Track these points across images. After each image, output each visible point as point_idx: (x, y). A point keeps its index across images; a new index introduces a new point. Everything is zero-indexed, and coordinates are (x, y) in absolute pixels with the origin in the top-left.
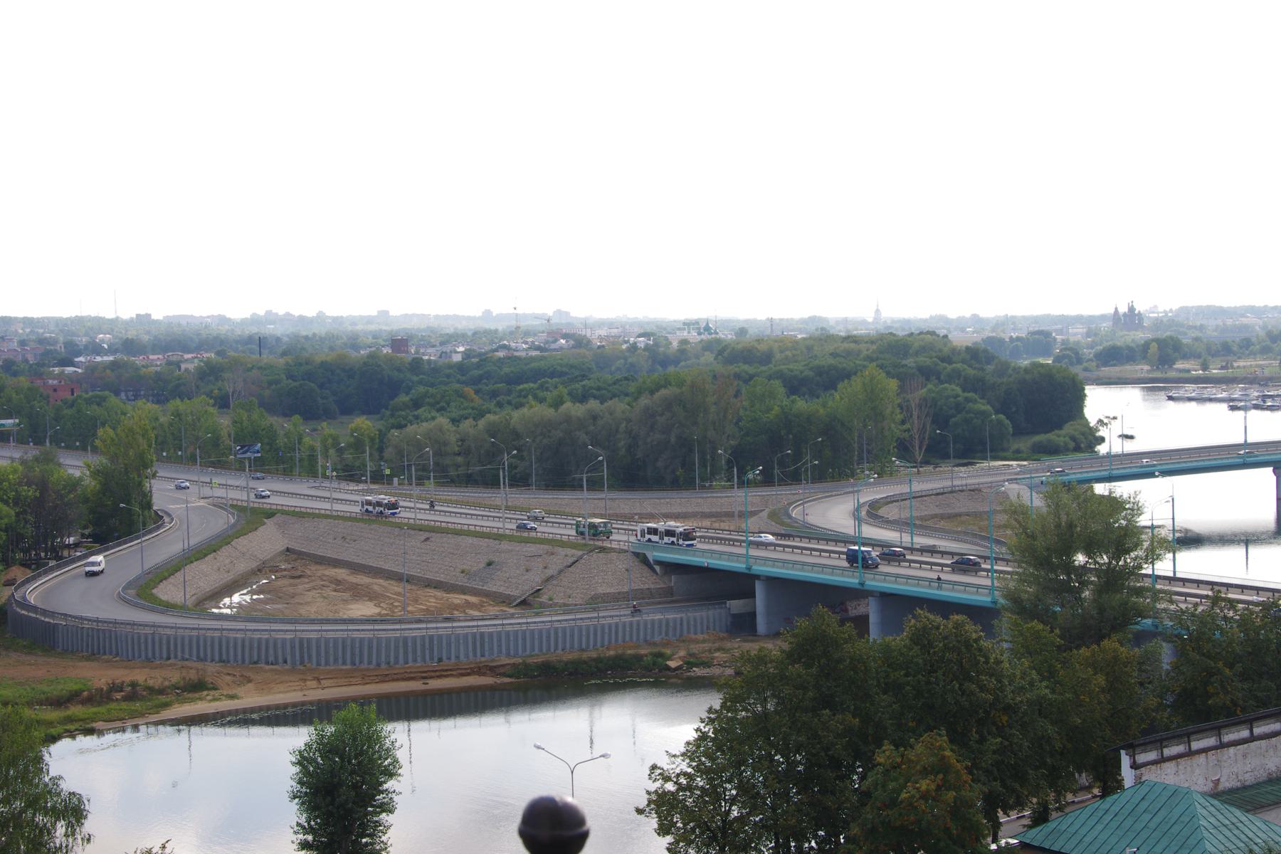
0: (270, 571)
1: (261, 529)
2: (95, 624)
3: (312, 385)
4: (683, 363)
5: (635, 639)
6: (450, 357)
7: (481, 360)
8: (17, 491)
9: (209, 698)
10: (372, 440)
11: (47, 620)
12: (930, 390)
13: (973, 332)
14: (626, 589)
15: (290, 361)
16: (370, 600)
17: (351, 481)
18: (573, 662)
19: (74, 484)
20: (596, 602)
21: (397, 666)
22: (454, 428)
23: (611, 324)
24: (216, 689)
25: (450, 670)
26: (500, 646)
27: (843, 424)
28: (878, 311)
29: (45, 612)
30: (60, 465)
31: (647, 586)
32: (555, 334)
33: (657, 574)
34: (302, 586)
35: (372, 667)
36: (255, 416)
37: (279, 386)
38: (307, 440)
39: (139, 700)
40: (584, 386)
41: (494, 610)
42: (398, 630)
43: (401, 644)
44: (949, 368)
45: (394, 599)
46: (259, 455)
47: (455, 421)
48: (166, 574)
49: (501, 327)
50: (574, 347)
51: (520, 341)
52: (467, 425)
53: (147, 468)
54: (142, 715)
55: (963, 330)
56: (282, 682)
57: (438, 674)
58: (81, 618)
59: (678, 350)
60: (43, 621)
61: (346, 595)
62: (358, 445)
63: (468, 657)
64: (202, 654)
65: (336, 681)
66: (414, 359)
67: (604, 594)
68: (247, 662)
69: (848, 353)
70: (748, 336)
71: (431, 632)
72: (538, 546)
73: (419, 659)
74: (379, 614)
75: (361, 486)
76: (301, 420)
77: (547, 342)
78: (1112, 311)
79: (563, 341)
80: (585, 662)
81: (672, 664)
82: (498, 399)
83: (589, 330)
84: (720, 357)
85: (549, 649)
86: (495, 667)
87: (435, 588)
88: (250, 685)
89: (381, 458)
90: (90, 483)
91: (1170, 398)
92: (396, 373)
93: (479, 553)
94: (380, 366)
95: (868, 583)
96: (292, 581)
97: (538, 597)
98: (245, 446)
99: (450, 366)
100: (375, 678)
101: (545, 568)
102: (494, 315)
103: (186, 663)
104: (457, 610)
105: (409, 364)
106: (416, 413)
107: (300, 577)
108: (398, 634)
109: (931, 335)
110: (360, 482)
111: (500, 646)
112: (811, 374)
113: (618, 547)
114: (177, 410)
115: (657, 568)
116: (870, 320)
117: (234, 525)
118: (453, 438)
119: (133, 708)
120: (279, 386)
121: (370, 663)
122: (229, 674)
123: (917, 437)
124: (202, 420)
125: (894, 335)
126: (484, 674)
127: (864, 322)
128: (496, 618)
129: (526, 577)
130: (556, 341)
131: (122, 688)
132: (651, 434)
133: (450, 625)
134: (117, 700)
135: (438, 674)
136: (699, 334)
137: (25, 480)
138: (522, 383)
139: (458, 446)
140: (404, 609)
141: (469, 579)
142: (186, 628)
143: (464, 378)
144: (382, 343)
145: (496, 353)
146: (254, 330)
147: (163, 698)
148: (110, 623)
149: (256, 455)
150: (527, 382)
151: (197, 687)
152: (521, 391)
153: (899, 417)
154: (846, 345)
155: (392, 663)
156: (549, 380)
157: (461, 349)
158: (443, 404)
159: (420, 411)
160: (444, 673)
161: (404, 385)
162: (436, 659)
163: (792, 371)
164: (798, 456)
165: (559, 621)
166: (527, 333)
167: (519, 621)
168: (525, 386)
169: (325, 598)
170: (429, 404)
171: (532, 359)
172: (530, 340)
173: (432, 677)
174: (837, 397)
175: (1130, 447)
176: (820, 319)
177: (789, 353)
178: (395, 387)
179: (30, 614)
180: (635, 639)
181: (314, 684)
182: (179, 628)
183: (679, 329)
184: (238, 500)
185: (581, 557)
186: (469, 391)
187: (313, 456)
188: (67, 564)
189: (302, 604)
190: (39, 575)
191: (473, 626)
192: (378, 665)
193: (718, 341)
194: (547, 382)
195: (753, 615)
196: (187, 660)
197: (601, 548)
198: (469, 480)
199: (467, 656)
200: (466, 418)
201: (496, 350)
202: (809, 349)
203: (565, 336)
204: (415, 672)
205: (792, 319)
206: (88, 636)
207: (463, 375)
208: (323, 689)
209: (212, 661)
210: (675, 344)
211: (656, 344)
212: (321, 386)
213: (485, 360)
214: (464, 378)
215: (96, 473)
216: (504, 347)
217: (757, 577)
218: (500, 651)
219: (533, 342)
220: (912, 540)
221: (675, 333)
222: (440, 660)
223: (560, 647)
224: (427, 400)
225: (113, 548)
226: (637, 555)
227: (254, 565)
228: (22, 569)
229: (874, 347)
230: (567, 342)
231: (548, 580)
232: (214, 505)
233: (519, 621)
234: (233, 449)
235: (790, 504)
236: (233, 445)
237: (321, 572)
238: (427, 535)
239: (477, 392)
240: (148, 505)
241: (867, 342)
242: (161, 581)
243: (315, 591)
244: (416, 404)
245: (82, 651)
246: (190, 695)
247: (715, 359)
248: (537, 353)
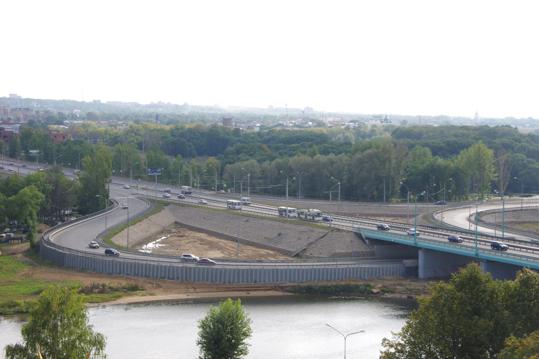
0: (167, 233)
1: (163, 211)
2: (84, 254)
3: (185, 140)
4: (373, 137)
5: (355, 277)
6: (253, 128)
7: (270, 131)
8: (44, 186)
9: (140, 294)
10: (217, 169)
11: (60, 251)
12: (508, 156)
13: (529, 127)
14: (350, 251)
15: (173, 128)
16: (219, 250)
17: (206, 189)
18: (323, 287)
19: (70, 184)
20: (335, 256)
21: (234, 283)
22: (259, 165)
23: (335, 115)
24: (144, 290)
25: (261, 287)
26: (286, 276)
27: (463, 172)
28: (477, 114)
29: (59, 247)
30: (63, 174)
31: (361, 250)
32: (307, 119)
33: (367, 244)
34: (184, 241)
35: (221, 283)
36: (158, 154)
37: (167, 140)
38: (184, 167)
39: (106, 293)
41: (282, 258)
42: (235, 265)
43: (236, 273)
44: (519, 145)
45: (230, 250)
46: (160, 174)
48: (117, 231)
49: (278, 114)
50: (316, 126)
51: (288, 122)
53: (107, 178)
54: (108, 301)
55: (524, 125)
56: (176, 289)
57: (254, 289)
58: (77, 251)
59: (371, 130)
60: (59, 252)
61: (207, 247)
62: (210, 172)
63: (270, 281)
64: (136, 273)
65: (203, 289)
66: (235, 129)
67: (339, 253)
68: (159, 277)
69: (463, 135)
70: (407, 124)
71: (252, 267)
72: (305, 226)
73: (245, 281)
74: (224, 257)
75: (212, 192)
76: (182, 157)
77: (302, 123)
79: (311, 123)
80: (329, 287)
82: (280, 151)
83: (324, 118)
84: (394, 134)
85: (311, 280)
86: (283, 287)
87: (251, 245)
88: (161, 289)
89: (222, 179)
90: (78, 183)
92: (226, 136)
93: (274, 229)
94: (218, 132)
95: (480, 254)
96: (179, 238)
97: (304, 253)
98: (153, 169)
99: (254, 134)
100: (223, 289)
101: (309, 238)
102: (274, 108)
103: (128, 276)
104: (263, 257)
105: (233, 131)
106: (238, 156)
107: (182, 236)
108: (235, 267)
109: (508, 127)
110: (211, 190)
111: (286, 276)
112: (444, 145)
113: (346, 229)
114: (119, 149)
115: (367, 241)
116: (473, 118)
117: (149, 209)
118: (258, 170)
119: (103, 297)
120: (167, 140)
121: (220, 281)
122: (150, 283)
123: (502, 180)
124: (132, 155)
125: (488, 127)
126: (278, 290)
127: (469, 119)
128: (283, 262)
129: (299, 242)
130: (307, 123)
131: (98, 287)
132: (361, 172)
133: (261, 264)
134: (95, 292)
135: (254, 289)
136: (382, 122)
137: (48, 181)
138: (292, 144)
139: (261, 174)
140: (237, 255)
141: (269, 242)
142: (129, 259)
143: (261, 140)
144: (218, 120)
145: (276, 128)
148: (92, 254)
149: (158, 174)
150: (294, 143)
151: (134, 289)
152: (291, 147)
153: (493, 170)
154: (462, 131)
155: (231, 282)
156: (306, 142)
157: (258, 125)
158: (252, 152)
159: (240, 156)
160: (257, 289)
161: (230, 142)
162: (253, 281)
163: (433, 143)
164: (437, 188)
165: (316, 265)
166: (291, 118)
167: (295, 265)
168: (294, 145)
169: (196, 247)
170: (244, 152)
172: (293, 122)
173: (251, 290)
174: (460, 157)
176: (446, 117)
177: (431, 134)
178: (225, 143)
179: (52, 248)
180: (355, 277)
181: (192, 290)
182: (126, 258)
183: (371, 119)
184: (150, 196)
185: (327, 234)
186: (265, 146)
187: (187, 175)
188: (68, 224)
189: (184, 250)
190: (55, 229)
191: (273, 266)
192: (225, 282)
193: (393, 126)
194: (305, 144)
196: (129, 275)
197: (337, 229)
198: (266, 192)
199: (269, 281)
200: (264, 160)
201: (276, 126)
202: (442, 132)
203: (312, 121)
204: (243, 287)
205: (430, 116)
206: (80, 260)
207: (260, 138)
208: (197, 293)
209: (142, 276)
210: (369, 127)
211: (359, 127)
212: (188, 141)
213: (272, 131)
214: (261, 140)
215: (81, 180)
216: (280, 125)
217: (420, 248)
218: (286, 279)
219: (295, 123)
220: (503, 234)
221: (369, 121)
222: (256, 282)
223: (317, 279)
224: (244, 150)
225: (90, 217)
226: (356, 234)
227: (159, 229)
228: (45, 225)
229: (477, 132)
230: (312, 123)
231: (310, 244)
232: (139, 198)
233: (295, 265)
234: (147, 171)
235: (434, 212)
236: (147, 168)
237: (193, 234)
238: (247, 218)
239: (269, 147)
240: (107, 197)
241: (473, 130)
242: (115, 235)
243: (190, 244)
244: (238, 152)
245: (77, 268)
246: (131, 292)
247: (391, 136)
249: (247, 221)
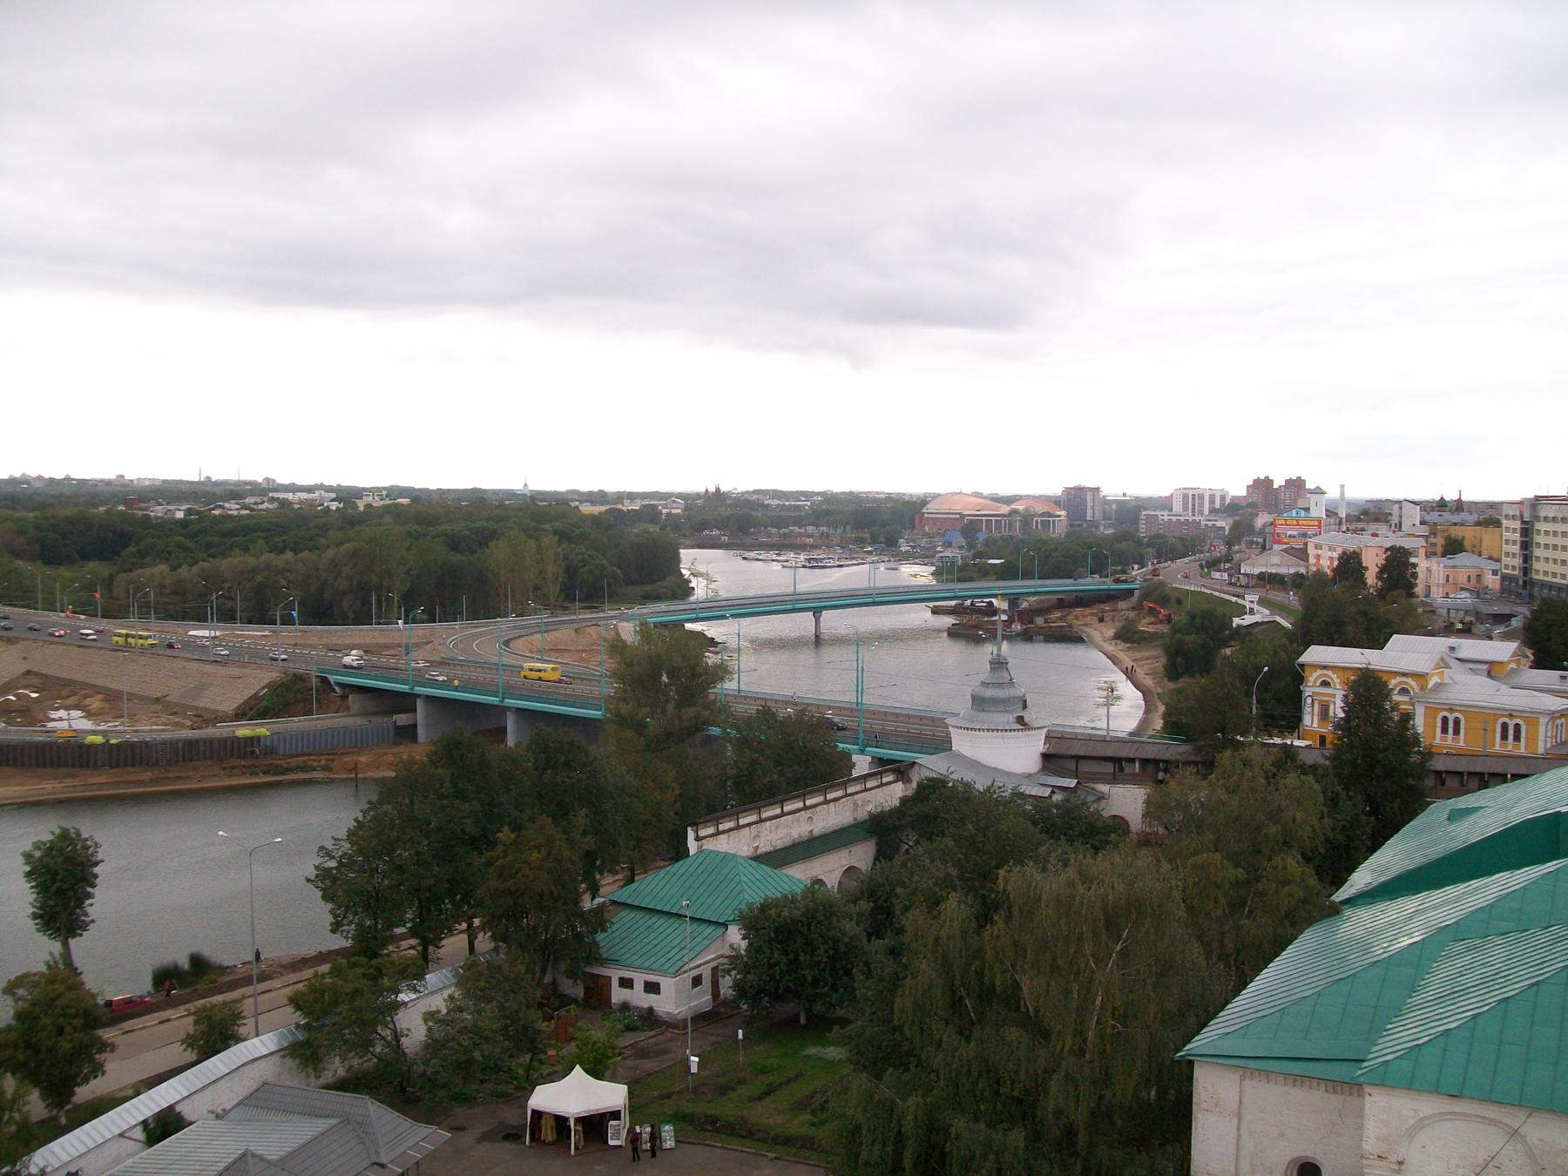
28: (526, 485)
40: (284, 541)
47: (174, 569)
52: (184, 571)
78: (704, 490)
91: (745, 558)
146: (9, 489)
171: (241, 517)
195: (415, 726)
217: (418, 696)
248: (248, 512)
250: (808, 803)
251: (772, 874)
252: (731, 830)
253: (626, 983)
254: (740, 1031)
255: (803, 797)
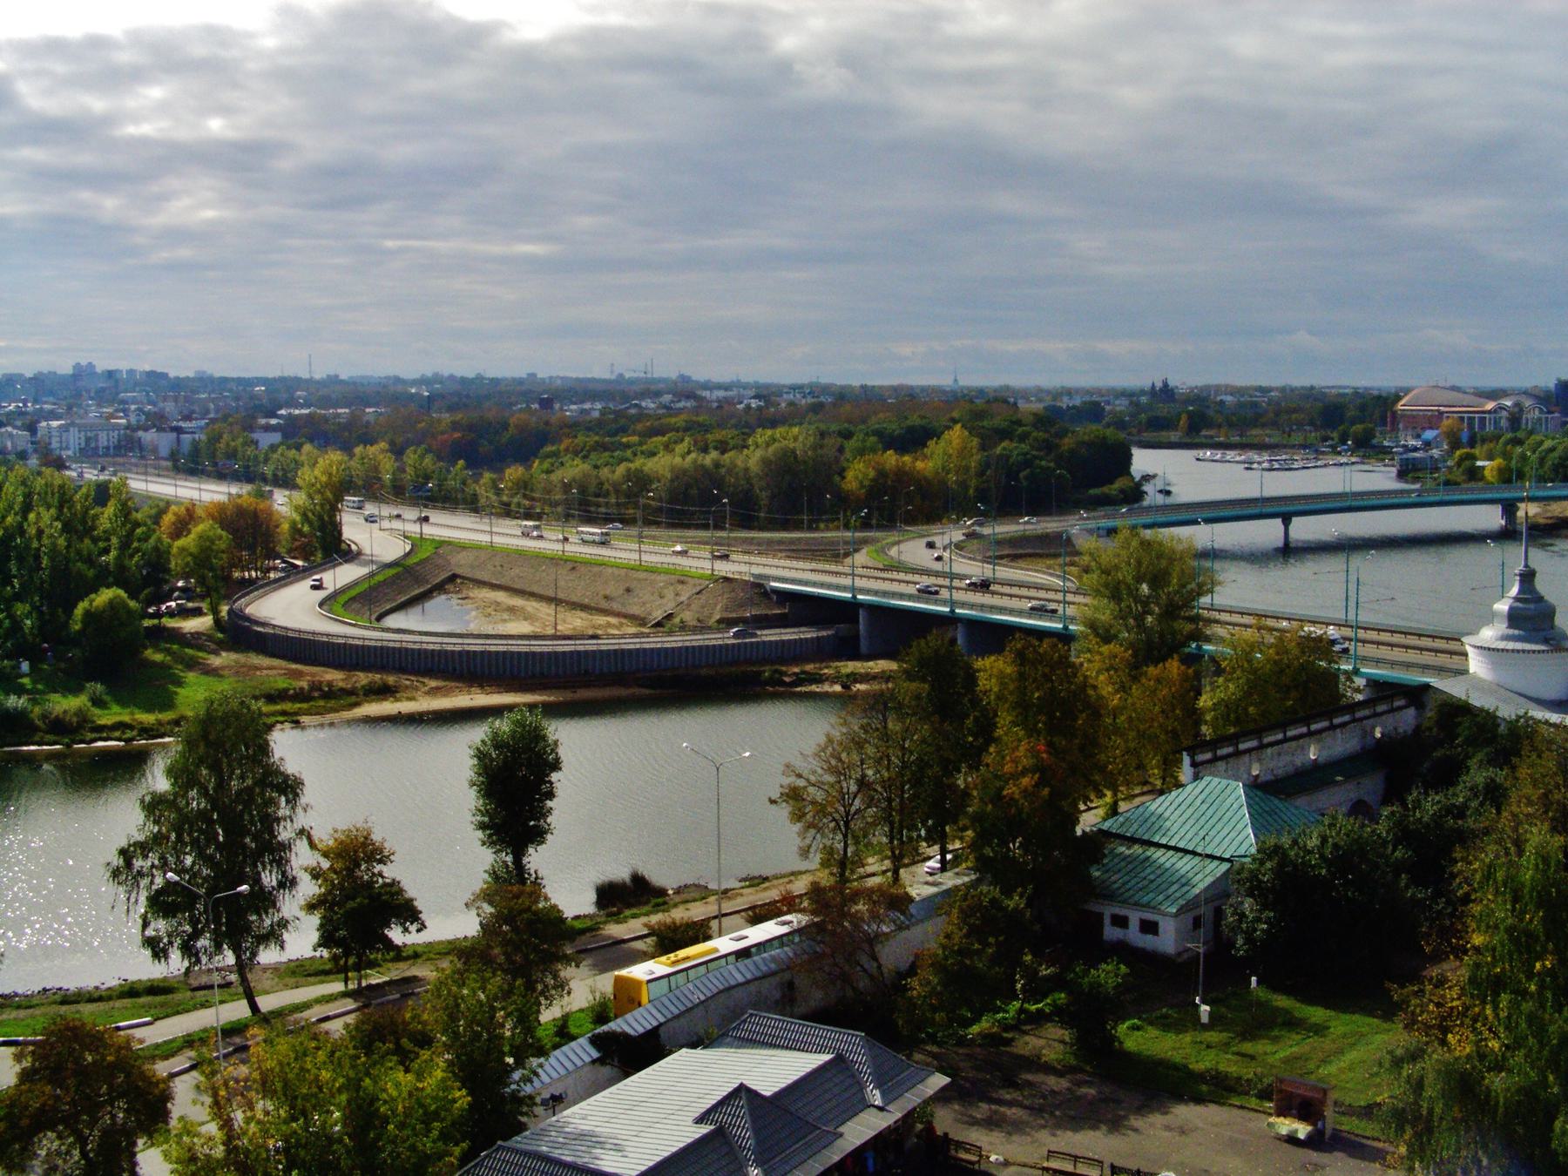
16: (525, 619)
61: (505, 616)
81: (787, 679)
147: (353, 699)
175: (1170, 500)
195: (856, 637)
249: (574, 568)
250: (1314, 727)
251: (1281, 806)
252: (1229, 756)
253: (1121, 922)
254: (1254, 979)
255: (1307, 721)
